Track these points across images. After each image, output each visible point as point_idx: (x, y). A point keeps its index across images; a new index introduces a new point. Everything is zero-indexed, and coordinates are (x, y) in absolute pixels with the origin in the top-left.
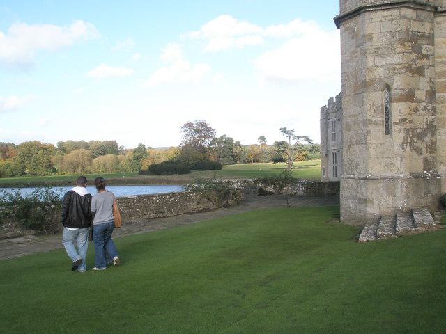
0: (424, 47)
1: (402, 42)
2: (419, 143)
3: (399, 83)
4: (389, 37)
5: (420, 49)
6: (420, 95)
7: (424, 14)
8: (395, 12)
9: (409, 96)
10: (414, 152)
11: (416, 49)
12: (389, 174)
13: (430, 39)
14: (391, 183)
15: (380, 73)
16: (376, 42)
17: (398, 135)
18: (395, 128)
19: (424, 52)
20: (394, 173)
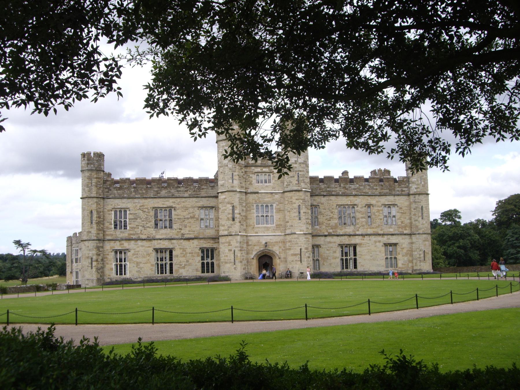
2: (99, 271)
3: (95, 258)
6: (99, 260)
7: (100, 242)
8: (94, 241)
9: (97, 261)
11: (99, 250)
13: (102, 247)
14: (92, 280)
15: (91, 255)
16: (90, 248)
17: (94, 269)
18: (93, 268)
20: (93, 278)
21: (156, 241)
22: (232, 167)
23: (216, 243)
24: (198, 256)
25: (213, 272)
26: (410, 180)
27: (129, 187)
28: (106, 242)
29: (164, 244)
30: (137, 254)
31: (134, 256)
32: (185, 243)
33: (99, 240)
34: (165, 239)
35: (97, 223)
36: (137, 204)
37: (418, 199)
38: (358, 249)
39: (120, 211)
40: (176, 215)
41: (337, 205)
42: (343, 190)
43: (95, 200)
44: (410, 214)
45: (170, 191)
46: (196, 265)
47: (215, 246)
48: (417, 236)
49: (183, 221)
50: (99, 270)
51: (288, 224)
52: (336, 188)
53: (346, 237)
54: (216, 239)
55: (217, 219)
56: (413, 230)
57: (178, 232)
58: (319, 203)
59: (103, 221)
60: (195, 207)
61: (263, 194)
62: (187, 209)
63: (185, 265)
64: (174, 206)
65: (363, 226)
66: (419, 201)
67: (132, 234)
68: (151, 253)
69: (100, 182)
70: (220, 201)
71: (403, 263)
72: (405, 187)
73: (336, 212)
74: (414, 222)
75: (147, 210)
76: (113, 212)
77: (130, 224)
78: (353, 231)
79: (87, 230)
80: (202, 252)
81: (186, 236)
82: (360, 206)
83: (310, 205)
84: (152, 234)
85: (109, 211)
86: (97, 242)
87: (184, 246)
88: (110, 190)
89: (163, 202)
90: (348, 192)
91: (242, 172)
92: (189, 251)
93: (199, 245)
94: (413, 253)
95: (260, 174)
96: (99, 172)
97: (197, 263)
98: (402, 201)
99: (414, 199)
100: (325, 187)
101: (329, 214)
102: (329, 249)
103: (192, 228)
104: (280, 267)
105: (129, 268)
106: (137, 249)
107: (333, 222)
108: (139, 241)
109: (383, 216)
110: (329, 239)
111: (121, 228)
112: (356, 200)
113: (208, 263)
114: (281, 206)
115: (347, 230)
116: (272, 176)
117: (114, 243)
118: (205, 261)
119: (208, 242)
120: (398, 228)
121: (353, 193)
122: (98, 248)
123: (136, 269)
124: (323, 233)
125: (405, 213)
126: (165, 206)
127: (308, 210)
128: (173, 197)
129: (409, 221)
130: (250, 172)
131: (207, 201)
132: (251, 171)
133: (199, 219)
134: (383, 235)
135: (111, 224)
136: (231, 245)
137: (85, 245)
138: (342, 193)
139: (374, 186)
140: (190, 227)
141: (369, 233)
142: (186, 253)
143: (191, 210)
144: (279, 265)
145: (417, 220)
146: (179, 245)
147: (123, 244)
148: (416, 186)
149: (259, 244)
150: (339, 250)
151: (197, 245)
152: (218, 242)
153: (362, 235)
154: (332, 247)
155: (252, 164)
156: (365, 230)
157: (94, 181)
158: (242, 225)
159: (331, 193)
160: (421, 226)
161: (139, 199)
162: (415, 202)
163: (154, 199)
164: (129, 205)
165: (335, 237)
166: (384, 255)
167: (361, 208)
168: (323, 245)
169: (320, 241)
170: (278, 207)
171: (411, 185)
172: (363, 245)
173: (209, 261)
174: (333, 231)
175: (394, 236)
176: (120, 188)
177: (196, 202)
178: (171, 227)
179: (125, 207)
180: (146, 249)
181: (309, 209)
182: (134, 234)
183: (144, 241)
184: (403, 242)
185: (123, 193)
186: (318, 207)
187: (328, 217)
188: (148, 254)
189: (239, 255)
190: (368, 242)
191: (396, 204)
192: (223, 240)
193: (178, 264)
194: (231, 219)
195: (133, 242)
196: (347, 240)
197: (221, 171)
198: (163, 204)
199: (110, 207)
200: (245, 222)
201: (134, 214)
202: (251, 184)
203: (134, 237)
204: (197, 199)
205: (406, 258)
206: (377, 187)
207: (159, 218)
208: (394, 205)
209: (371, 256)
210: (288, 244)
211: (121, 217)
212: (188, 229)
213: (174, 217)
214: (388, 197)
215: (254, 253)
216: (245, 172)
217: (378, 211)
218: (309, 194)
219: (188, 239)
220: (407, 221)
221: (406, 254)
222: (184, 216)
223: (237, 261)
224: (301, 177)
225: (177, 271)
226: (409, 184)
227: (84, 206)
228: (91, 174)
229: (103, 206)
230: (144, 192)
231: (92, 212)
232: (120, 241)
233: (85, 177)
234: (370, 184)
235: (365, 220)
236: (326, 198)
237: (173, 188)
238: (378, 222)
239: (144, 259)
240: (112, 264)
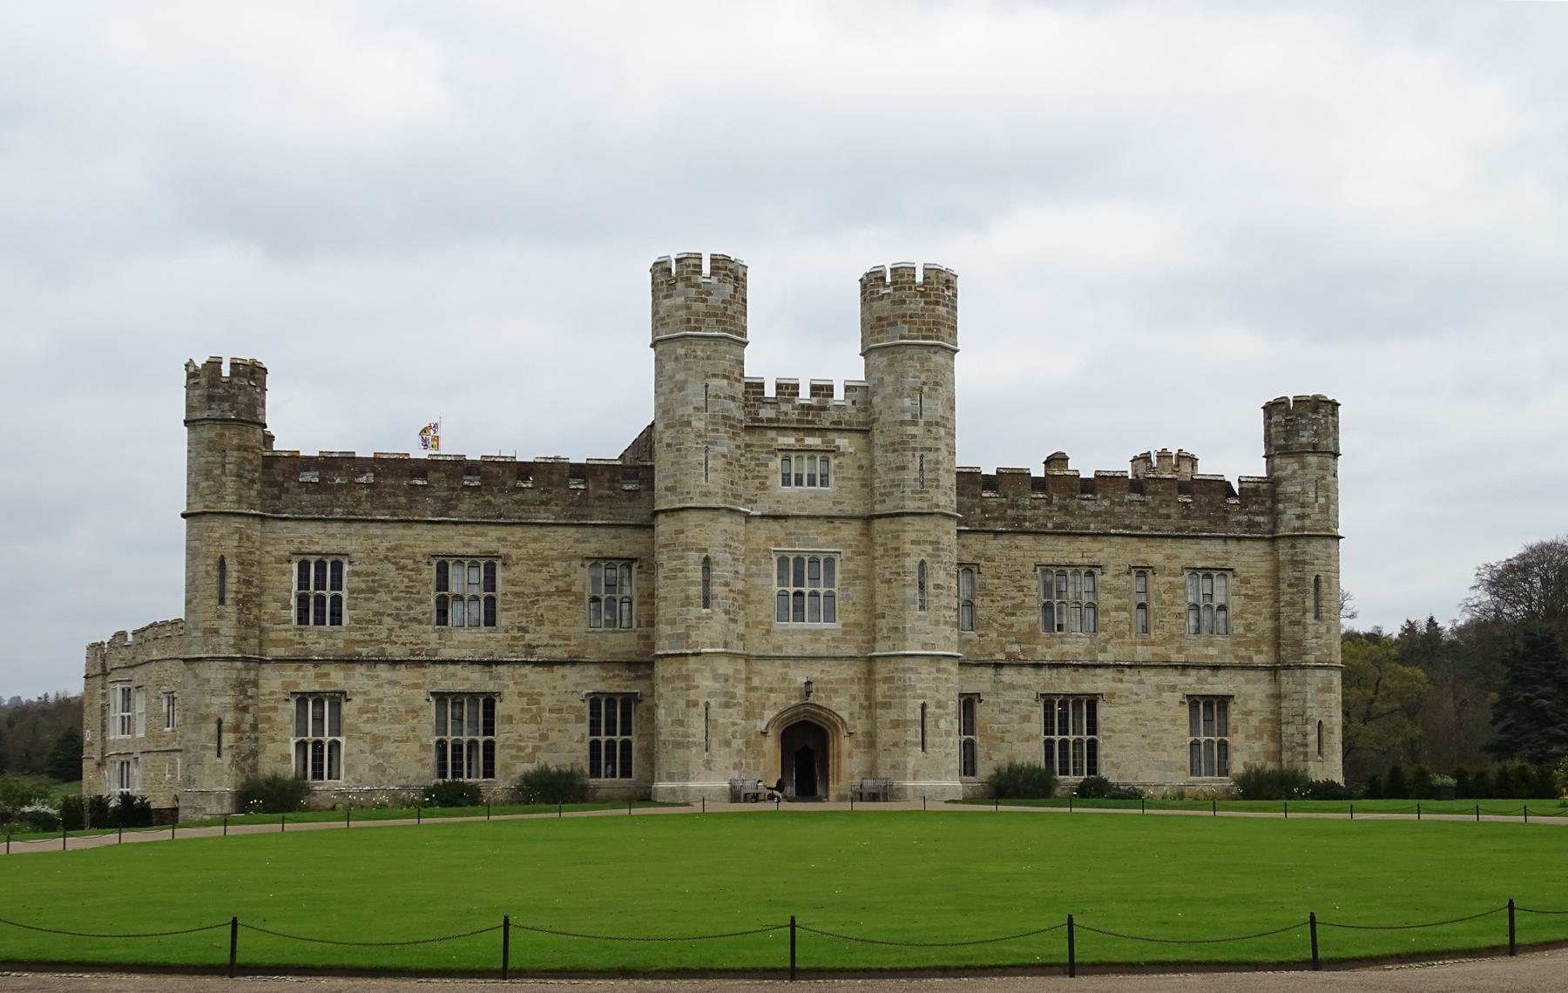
0: (249, 690)
1: (233, 687)
2: (243, 764)
3: (229, 719)
4: (222, 681)
5: (247, 691)
6: (246, 727)
7: (252, 664)
8: (228, 664)
9: (236, 728)
10: (238, 772)
11: (244, 692)
12: (218, 788)
13: (255, 684)
14: (220, 797)
15: (214, 709)
16: (213, 685)
17: (227, 758)
18: (224, 753)
19: (249, 694)
21: (439, 668)
22: (707, 430)
23: (638, 678)
24: (579, 720)
25: (626, 772)
26: (1280, 489)
27: (351, 481)
28: (267, 670)
29: (468, 679)
30: (375, 710)
31: (365, 717)
32: (536, 677)
33: (246, 660)
34: (472, 663)
35: (238, 602)
36: (376, 541)
37: (1304, 552)
38: (1102, 711)
39: (320, 566)
40: (508, 581)
41: (1036, 565)
42: (1058, 518)
43: (236, 523)
44: (1277, 601)
45: (489, 503)
46: (573, 751)
47: (636, 688)
48: (1298, 673)
49: (534, 603)
50: (244, 759)
51: (883, 624)
52: (1035, 508)
53: (1064, 670)
54: (642, 665)
55: (650, 598)
56: (1283, 653)
57: (514, 638)
58: (980, 558)
59: (262, 593)
60: (571, 558)
61: (803, 523)
62: (545, 562)
63: (536, 749)
64: (503, 551)
65: (1120, 635)
66: (1307, 558)
67: (358, 642)
68: (421, 708)
69: (251, 462)
70: (661, 540)
71: (1247, 759)
72: (1262, 514)
73: (1033, 587)
74: (1287, 629)
75: (409, 562)
76: (295, 567)
77: (349, 608)
78: (1089, 652)
79: (207, 624)
80: (592, 707)
81: (542, 654)
82: (1111, 571)
83: (955, 561)
84: (428, 643)
85: (279, 561)
86: (238, 664)
87: (532, 687)
88: (287, 491)
89: (466, 539)
90: (1074, 523)
91: (738, 447)
92: (548, 701)
93: (584, 684)
94: (1284, 727)
95: (793, 455)
96: (250, 427)
97: (573, 744)
98: (1250, 558)
99: (1291, 551)
100: (1001, 505)
101: (1015, 593)
102: (1007, 707)
103: (560, 628)
104: (848, 764)
105: (346, 755)
106: (375, 694)
107: (1021, 619)
108: (380, 666)
109: (1187, 607)
110: (1008, 675)
111: (320, 621)
112: (1100, 551)
113: (611, 745)
114: (860, 560)
115: (1066, 648)
116: (833, 462)
117: (298, 669)
118: (603, 738)
119: (614, 676)
120: (1233, 644)
121: (1092, 526)
122: (241, 686)
123: (371, 759)
124: (992, 655)
125: (1259, 598)
126: (471, 551)
127: (949, 579)
128: (498, 520)
129: (1269, 624)
130: (762, 446)
131: (614, 538)
132: (765, 442)
133: (587, 599)
134: (1184, 667)
135: (287, 607)
136: (698, 687)
137: (196, 676)
138: (1054, 524)
139: (1161, 505)
140: (555, 623)
141: (1139, 659)
142: (541, 710)
143: (560, 567)
144: (850, 756)
145: (1297, 623)
146: (516, 683)
147: (326, 675)
148: (1298, 511)
149: (786, 685)
150: (1039, 711)
151: (577, 685)
152: (649, 677)
153: (1116, 666)
154: (1017, 702)
155: (769, 420)
156: (1126, 649)
157: (233, 456)
158: (734, 621)
159: (1020, 526)
160: (1311, 642)
161: (385, 526)
162: (1294, 563)
163: (436, 527)
164: (350, 545)
165: (1028, 671)
166: (1186, 731)
167: (1115, 576)
168: (988, 694)
169: (981, 681)
170: (851, 566)
171: (1281, 506)
172: (1120, 697)
173: (618, 738)
174: (1023, 651)
175: (1221, 673)
176: (321, 487)
177: (577, 541)
178: (490, 620)
179: (337, 551)
180: (407, 692)
181: (951, 576)
182: (365, 643)
183: (398, 667)
184: (1250, 693)
185: (333, 506)
186: (975, 569)
187: (1009, 603)
188: (413, 711)
189: (721, 721)
190: (1135, 688)
191: (1229, 566)
192: (670, 668)
193: (512, 747)
194: (701, 601)
195: (360, 669)
196: (1068, 679)
197: (669, 441)
198: (466, 545)
199: (284, 549)
200: (742, 613)
201: (368, 575)
202: (763, 486)
203: (365, 651)
204: (581, 530)
205: (1257, 746)
206: (1172, 511)
207: (454, 588)
208: (1224, 571)
209: (1143, 736)
210: (881, 690)
211: (320, 584)
212: (547, 629)
213: (500, 587)
214: (1206, 544)
215: (770, 714)
216: (747, 446)
217: (1172, 588)
218: (952, 526)
219: (549, 664)
220: (1265, 625)
221: (1258, 735)
222: (536, 588)
223: (714, 741)
224: (931, 471)
225: (506, 766)
226: (1276, 501)
227: (194, 543)
228: (222, 435)
229: (262, 543)
230: (403, 500)
231: (222, 563)
232: (316, 663)
233: (199, 442)
234: (1149, 498)
235: (1124, 615)
236: (1004, 541)
237: (501, 491)
238: (1170, 623)
239: (397, 726)
240: (287, 741)
